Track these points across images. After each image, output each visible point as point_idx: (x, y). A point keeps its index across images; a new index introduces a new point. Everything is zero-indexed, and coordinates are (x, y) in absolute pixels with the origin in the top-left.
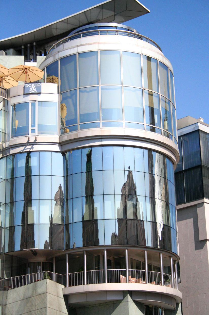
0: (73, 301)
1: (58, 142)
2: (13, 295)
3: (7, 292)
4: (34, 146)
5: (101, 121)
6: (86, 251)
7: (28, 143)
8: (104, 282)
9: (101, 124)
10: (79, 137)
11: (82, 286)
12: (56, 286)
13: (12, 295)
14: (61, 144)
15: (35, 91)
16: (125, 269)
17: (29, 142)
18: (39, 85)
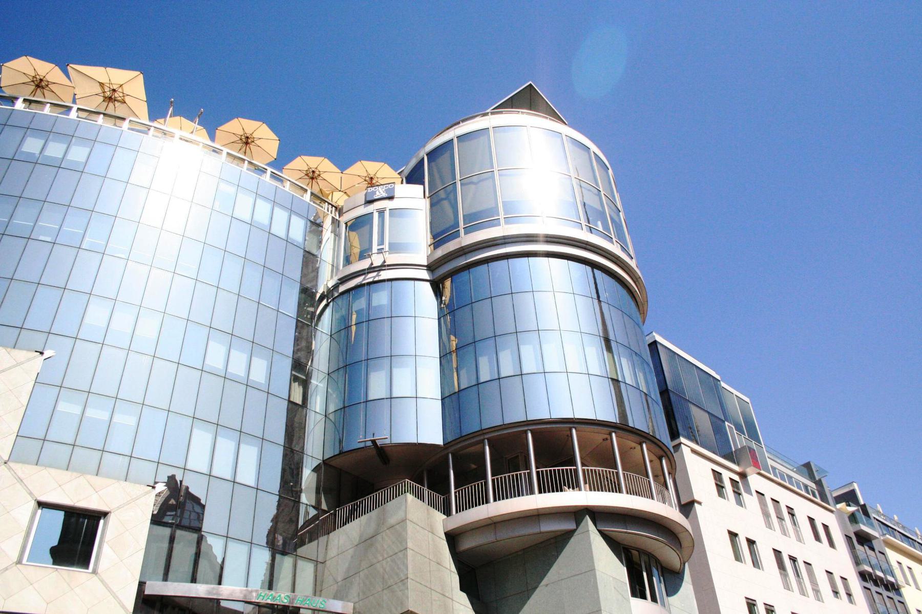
0: (467, 544)
1: (426, 264)
2: (339, 541)
3: (328, 538)
4: (382, 273)
5: (502, 216)
6: (488, 439)
7: (372, 269)
8: (532, 493)
9: (502, 221)
10: (463, 245)
11: (485, 505)
12: (428, 513)
13: (336, 542)
14: (432, 268)
15: (384, 195)
16: (575, 467)
17: (373, 266)
18: (391, 186)
